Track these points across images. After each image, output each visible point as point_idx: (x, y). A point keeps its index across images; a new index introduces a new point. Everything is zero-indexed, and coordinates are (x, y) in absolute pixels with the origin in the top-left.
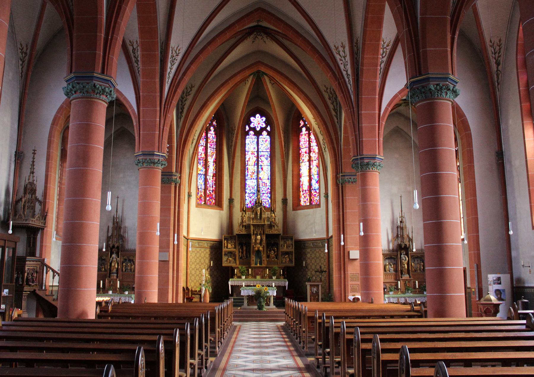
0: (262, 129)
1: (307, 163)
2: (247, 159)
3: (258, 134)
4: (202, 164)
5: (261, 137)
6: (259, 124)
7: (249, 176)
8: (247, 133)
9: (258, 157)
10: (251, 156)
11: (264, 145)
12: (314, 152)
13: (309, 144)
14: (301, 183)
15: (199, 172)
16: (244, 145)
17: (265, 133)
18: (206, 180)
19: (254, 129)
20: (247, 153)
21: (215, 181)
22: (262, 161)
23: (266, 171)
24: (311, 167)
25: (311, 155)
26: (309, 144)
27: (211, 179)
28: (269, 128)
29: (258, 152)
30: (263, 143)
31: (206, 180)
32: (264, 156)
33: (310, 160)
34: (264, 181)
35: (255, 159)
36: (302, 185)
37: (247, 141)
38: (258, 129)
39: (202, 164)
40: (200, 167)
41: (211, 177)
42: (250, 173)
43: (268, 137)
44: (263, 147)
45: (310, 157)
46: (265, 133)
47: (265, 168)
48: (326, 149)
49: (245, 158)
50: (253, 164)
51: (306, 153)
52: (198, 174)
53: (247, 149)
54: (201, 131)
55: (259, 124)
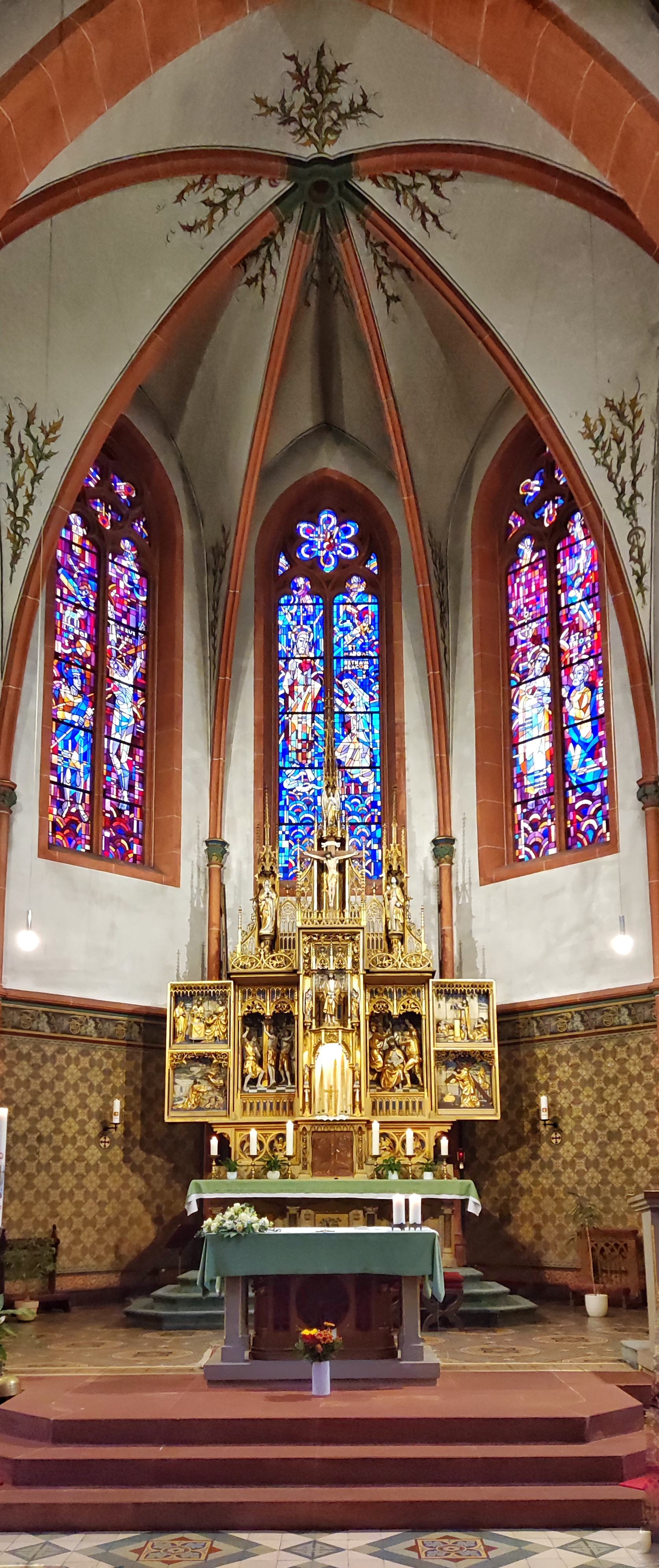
0: (345, 569)
1: (545, 683)
2: (285, 688)
3: (328, 589)
4: (77, 683)
5: (340, 598)
6: (332, 547)
7: (293, 755)
8: (286, 585)
9: (328, 681)
10: (300, 677)
11: (356, 632)
12: (574, 628)
13: (554, 601)
14: (516, 771)
15: (60, 715)
16: (270, 632)
17: (356, 585)
18: (96, 757)
19: (312, 568)
20: (281, 663)
21: (142, 766)
22: (347, 697)
23: (362, 736)
24: (564, 693)
25: (563, 643)
26: (554, 601)
27: (125, 757)
28: (373, 564)
29: (328, 658)
30: (348, 623)
31: (96, 757)
32: (353, 674)
33: (557, 668)
34: (355, 774)
35: (317, 686)
36: (521, 777)
37: (285, 618)
38: (329, 568)
39: (77, 683)
40: (69, 695)
41: (125, 749)
42: (294, 744)
43: (370, 599)
44: (348, 638)
45: (557, 653)
46: (356, 585)
47: (358, 723)
48: (646, 580)
49: (277, 684)
50: (309, 709)
51: (536, 640)
52: (50, 720)
53: (282, 647)
54: (58, 499)
55: (332, 547)
